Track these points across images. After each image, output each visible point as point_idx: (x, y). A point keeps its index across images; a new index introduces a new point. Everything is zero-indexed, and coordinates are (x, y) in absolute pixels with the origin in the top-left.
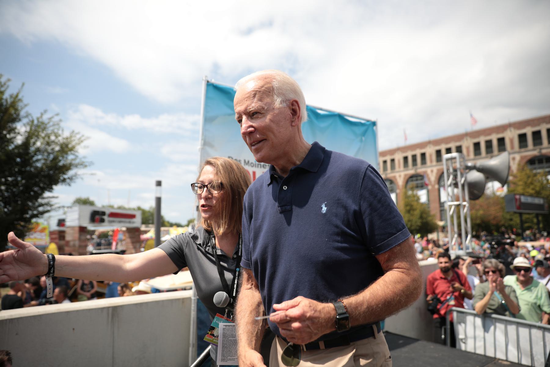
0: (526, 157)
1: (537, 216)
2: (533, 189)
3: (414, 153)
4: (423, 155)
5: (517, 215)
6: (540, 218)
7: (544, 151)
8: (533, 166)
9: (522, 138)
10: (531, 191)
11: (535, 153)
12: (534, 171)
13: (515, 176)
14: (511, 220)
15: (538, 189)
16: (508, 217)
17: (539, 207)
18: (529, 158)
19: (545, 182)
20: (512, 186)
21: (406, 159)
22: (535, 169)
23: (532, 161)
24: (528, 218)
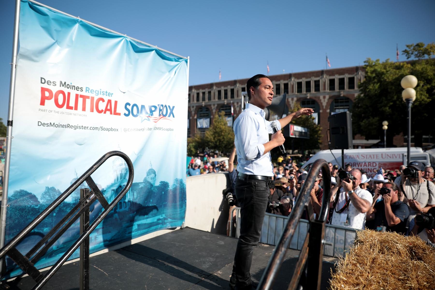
3: (226, 88)
4: (232, 91)
9: (300, 84)
21: (219, 92)
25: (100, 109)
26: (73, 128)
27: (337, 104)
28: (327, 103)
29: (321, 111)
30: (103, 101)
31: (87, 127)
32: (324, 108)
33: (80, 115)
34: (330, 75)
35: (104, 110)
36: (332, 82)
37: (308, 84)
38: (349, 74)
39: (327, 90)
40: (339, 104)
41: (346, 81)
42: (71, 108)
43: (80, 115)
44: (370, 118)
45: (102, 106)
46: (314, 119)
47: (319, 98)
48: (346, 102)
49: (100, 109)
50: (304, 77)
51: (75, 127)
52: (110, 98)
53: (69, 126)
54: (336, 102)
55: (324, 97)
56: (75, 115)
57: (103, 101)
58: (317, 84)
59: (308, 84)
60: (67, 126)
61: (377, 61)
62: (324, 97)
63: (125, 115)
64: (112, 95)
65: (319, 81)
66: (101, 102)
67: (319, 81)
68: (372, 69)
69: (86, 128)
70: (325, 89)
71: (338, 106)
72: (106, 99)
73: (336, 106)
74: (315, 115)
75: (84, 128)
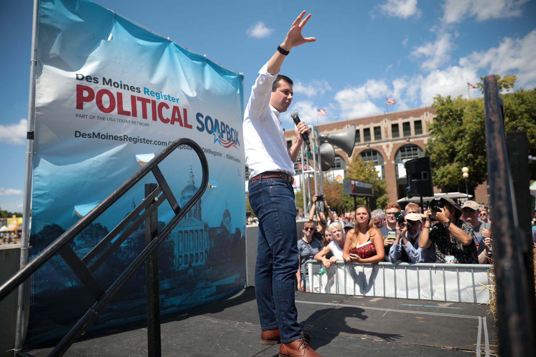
0: (359, 149)
1: (366, 199)
2: (364, 176)
5: (353, 198)
6: (368, 200)
7: (371, 146)
8: (364, 158)
10: (362, 178)
11: (365, 147)
12: (365, 162)
13: (351, 166)
14: (347, 202)
15: (367, 176)
16: (346, 200)
17: (369, 191)
18: (361, 151)
19: (373, 170)
20: (348, 174)
22: (365, 160)
23: (363, 154)
24: (360, 201)
25: (165, 118)
26: (133, 142)
27: (403, 153)
28: (392, 153)
29: (385, 163)
30: (168, 107)
31: (151, 141)
32: (389, 158)
33: (141, 124)
34: (392, 120)
35: (170, 118)
36: (395, 127)
37: (367, 131)
38: (415, 117)
39: (390, 138)
40: (406, 153)
41: (412, 125)
42: (127, 114)
43: (141, 124)
44: (446, 165)
45: (167, 113)
46: (378, 172)
47: (381, 147)
48: (414, 150)
49: (165, 118)
50: (361, 123)
51: (135, 140)
52: (175, 104)
53: (126, 139)
54: (402, 151)
55: (388, 146)
56: (134, 123)
57: (168, 107)
58: (377, 130)
59: (367, 131)
60: (123, 138)
61: (449, 97)
62: (388, 146)
63: (198, 128)
64: (178, 101)
65: (379, 127)
66: (164, 108)
67: (379, 127)
68: (443, 107)
69: (150, 143)
70: (387, 136)
71: (405, 156)
72: (171, 105)
73: (402, 156)
74: (378, 168)
75: (147, 141)
